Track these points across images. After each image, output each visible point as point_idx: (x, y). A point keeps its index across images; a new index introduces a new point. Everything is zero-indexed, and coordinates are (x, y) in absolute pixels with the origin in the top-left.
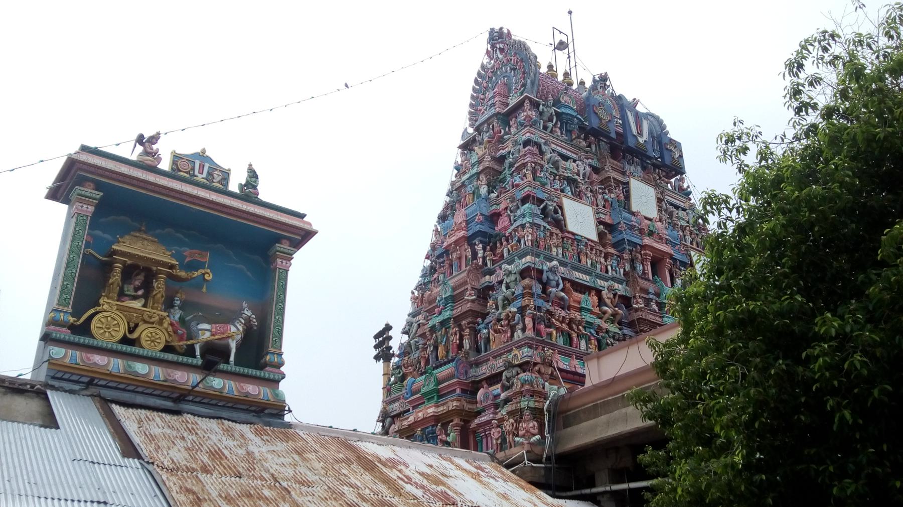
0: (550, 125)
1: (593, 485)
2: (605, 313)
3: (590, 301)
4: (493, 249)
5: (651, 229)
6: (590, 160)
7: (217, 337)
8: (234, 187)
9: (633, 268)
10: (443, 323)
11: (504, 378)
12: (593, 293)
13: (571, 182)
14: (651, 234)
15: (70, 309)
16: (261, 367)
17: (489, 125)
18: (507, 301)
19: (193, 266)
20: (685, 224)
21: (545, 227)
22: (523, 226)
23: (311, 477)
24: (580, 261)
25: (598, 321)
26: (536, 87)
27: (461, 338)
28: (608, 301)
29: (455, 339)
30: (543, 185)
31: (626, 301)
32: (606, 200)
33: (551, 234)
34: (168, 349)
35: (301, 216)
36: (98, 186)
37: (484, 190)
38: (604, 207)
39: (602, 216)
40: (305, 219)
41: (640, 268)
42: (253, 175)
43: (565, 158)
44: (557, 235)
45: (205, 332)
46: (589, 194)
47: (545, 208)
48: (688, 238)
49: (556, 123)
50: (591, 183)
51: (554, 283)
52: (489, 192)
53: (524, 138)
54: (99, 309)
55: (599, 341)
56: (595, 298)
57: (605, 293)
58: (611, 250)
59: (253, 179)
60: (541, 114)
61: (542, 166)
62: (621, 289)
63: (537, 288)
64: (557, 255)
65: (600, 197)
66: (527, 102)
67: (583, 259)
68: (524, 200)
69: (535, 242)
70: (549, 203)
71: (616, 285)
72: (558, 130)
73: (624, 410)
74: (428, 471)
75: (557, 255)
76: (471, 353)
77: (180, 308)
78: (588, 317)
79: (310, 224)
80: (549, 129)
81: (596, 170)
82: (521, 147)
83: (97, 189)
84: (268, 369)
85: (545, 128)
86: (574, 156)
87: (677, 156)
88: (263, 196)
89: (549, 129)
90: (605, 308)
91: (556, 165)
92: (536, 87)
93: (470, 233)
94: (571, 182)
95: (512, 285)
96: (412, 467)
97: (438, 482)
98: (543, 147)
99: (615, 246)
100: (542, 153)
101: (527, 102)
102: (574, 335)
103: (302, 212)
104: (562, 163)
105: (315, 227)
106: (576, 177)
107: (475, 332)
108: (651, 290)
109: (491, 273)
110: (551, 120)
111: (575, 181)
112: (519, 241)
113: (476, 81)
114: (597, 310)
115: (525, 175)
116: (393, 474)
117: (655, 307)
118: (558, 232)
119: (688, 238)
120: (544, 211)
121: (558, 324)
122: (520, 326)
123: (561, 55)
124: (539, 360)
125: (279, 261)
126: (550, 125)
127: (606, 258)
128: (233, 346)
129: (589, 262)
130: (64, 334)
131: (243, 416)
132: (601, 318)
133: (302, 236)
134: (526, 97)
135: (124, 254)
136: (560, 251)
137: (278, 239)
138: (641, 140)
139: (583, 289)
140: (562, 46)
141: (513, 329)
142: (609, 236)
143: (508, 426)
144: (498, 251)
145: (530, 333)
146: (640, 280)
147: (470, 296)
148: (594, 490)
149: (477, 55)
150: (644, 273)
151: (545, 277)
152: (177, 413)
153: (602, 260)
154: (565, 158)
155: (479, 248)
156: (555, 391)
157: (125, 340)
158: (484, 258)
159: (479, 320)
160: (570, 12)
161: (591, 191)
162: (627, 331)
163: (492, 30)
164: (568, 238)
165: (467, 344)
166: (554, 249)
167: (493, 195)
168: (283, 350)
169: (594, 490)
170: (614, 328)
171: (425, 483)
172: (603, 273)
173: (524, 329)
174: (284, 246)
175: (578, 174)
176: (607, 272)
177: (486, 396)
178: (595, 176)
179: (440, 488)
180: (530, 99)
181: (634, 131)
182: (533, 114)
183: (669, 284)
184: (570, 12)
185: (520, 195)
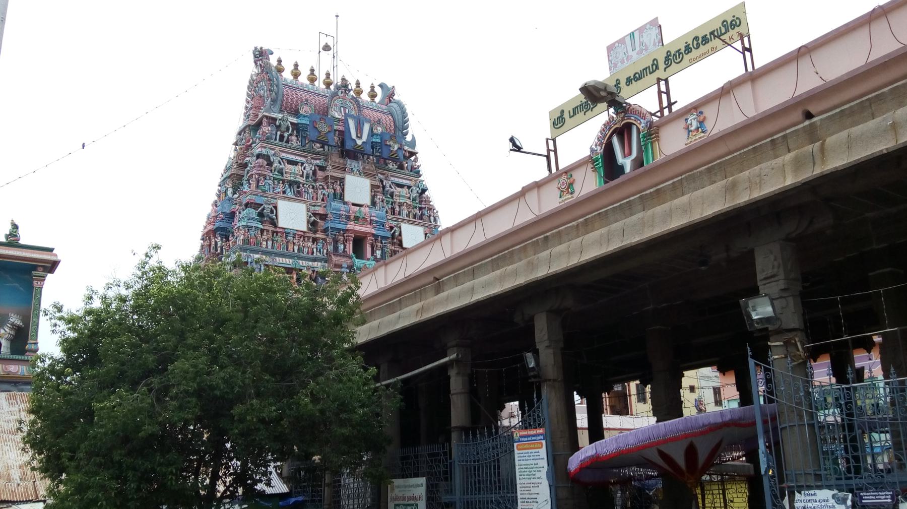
5: (358, 215)
6: (318, 161)
9: (336, 248)
13: (291, 184)
14: (356, 218)
21: (256, 228)
24: (287, 249)
26: (279, 102)
30: (264, 192)
33: (262, 231)
35: (51, 250)
37: (230, 191)
38: (323, 200)
39: (317, 208)
40: (54, 252)
41: (341, 247)
44: (268, 231)
46: (311, 190)
47: (264, 209)
48: (405, 212)
49: (293, 131)
50: (315, 181)
52: (234, 193)
60: (278, 127)
64: (267, 247)
65: (320, 192)
67: (290, 247)
68: (247, 205)
69: (247, 241)
72: (294, 138)
75: (267, 247)
79: (56, 255)
80: (285, 139)
81: (322, 168)
84: (28, 354)
85: (282, 137)
86: (303, 159)
87: (396, 148)
89: (285, 139)
91: (281, 172)
92: (279, 102)
93: (215, 227)
100: (270, 164)
103: (50, 247)
105: (59, 258)
111: (298, 184)
113: (248, 88)
118: (271, 228)
119: (405, 212)
120: (261, 215)
123: (327, 56)
125: (35, 282)
126: (286, 135)
129: (296, 248)
133: (52, 266)
136: (270, 243)
137: (35, 268)
138: (359, 142)
140: (327, 48)
149: (250, 69)
153: (310, 244)
158: (222, 248)
160: (337, 16)
161: (313, 188)
163: (256, 48)
167: (236, 196)
168: (39, 340)
172: (310, 255)
174: (39, 273)
175: (302, 176)
176: (313, 253)
184: (337, 16)
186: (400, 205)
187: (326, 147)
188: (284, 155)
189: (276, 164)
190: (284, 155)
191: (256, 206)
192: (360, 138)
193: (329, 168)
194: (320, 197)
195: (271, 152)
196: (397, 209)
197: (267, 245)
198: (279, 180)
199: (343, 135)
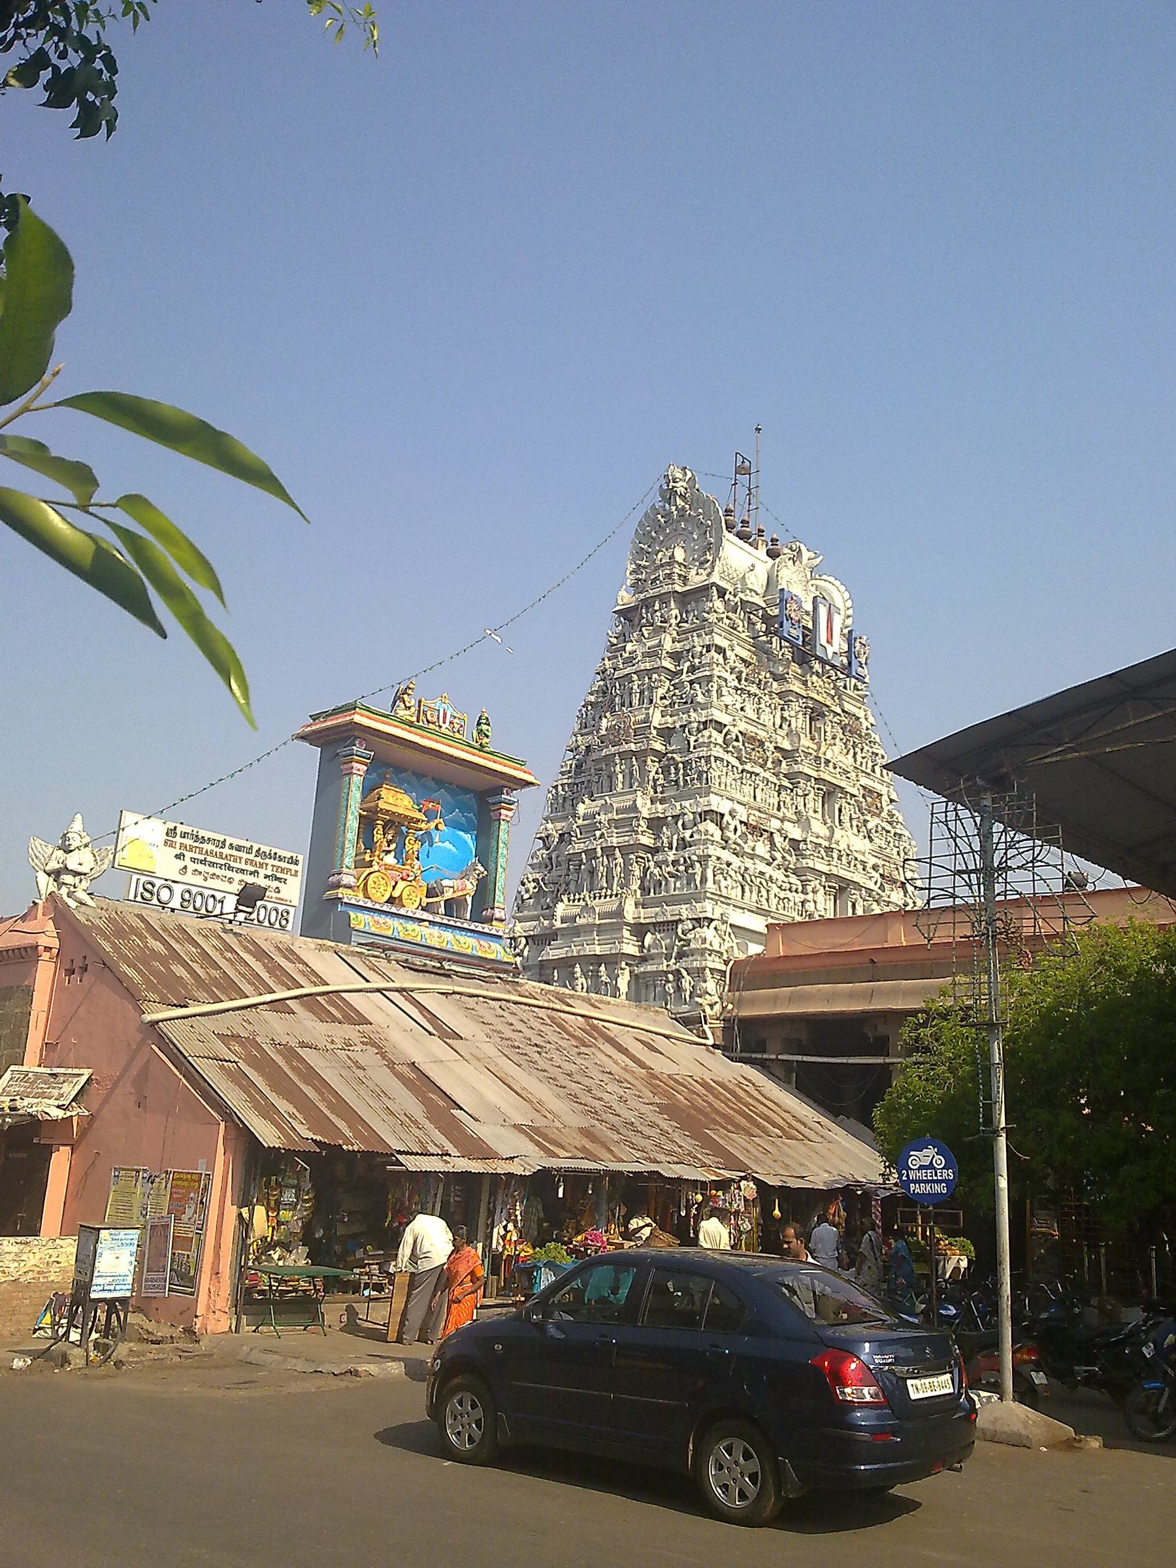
7: (460, 894)
16: (489, 920)
17: (661, 602)
19: (430, 815)
22: (708, 759)
32: (782, 718)
54: (372, 870)
57: (778, 839)
58: (786, 783)
62: (795, 833)
70: (732, 728)
71: (787, 826)
76: (639, 892)
98: (728, 653)
114: (767, 856)
132: (769, 864)
134: (714, 584)
151: (725, 821)
157: (391, 900)
164: (748, 772)
170: (779, 875)
177: (656, 944)
180: (718, 587)
182: (718, 604)
188: (738, 650)
190: (738, 650)
198: (737, 689)
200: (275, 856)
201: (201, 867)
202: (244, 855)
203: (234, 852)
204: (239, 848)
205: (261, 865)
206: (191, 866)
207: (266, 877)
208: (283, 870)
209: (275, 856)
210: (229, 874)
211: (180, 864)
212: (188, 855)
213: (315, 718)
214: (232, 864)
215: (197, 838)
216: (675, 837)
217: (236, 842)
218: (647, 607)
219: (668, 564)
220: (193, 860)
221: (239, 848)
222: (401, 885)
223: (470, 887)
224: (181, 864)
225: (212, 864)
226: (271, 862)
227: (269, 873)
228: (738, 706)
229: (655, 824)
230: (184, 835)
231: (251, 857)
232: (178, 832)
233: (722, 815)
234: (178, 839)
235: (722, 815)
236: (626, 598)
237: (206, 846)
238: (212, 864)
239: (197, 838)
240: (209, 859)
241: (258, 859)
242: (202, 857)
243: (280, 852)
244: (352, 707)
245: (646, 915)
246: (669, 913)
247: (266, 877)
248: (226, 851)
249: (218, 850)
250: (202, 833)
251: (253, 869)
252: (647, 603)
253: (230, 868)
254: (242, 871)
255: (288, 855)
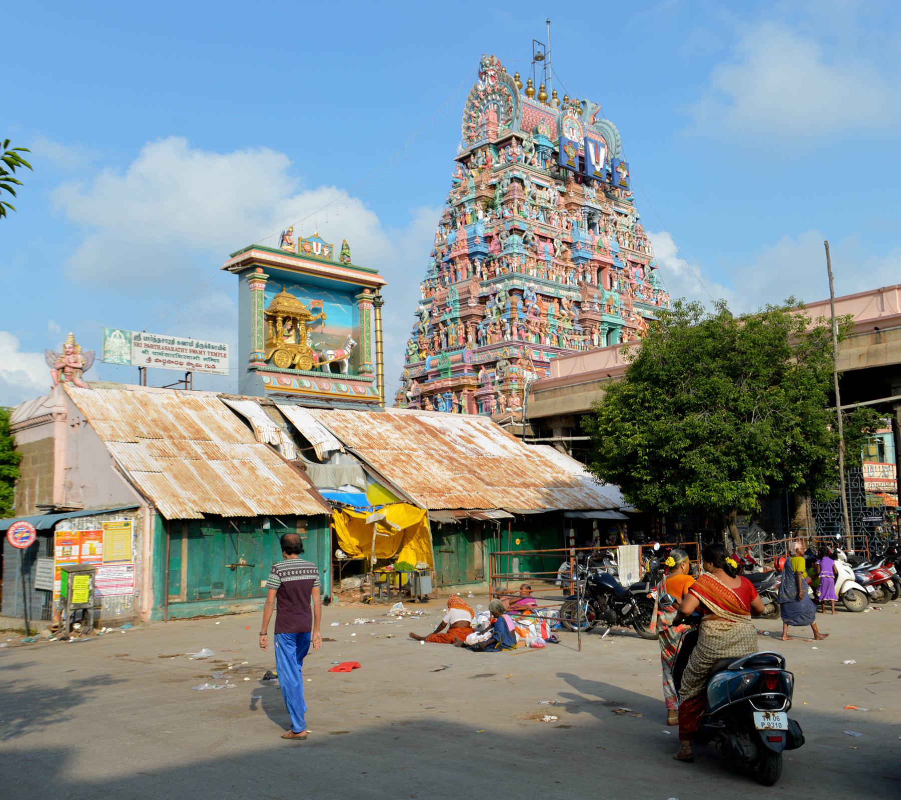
0: (530, 156)
1: (551, 436)
2: (563, 315)
3: (553, 307)
4: (488, 265)
8: (336, 258)
9: (585, 278)
10: (452, 320)
11: (498, 367)
12: (556, 300)
13: (544, 209)
15: (263, 351)
16: (359, 373)
18: (500, 312)
20: (625, 230)
22: (511, 254)
23: (415, 446)
25: (558, 323)
27: (466, 333)
28: (565, 306)
29: (462, 333)
31: (578, 304)
34: (313, 368)
36: (266, 271)
37: (480, 214)
39: (565, 237)
42: (345, 246)
43: (540, 187)
45: (331, 355)
46: (557, 217)
48: (627, 242)
51: (530, 298)
53: (511, 175)
55: (558, 337)
56: (558, 305)
57: (564, 301)
58: (571, 265)
59: (347, 251)
61: (524, 201)
63: (520, 304)
65: (564, 219)
66: (514, 140)
68: (511, 232)
71: (571, 293)
73: (572, 396)
74: (461, 433)
77: (311, 338)
78: (552, 321)
82: (509, 181)
83: (265, 273)
88: (354, 262)
89: (529, 161)
90: (563, 311)
94: (544, 209)
95: (503, 299)
96: (454, 432)
97: (470, 442)
98: (526, 182)
99: (572, 260)
101: (514, 140)
102: (542, 335)
104: (539, 193)
106: (548, 205)
107: (477, 331)
108: (596, 296)
109: (488, 285)
110: (531, 150)
112: (508, 266)
114: (557, 314)
115: (512, 209)
116: (448, 439)
117: (597, 308)
118: (534, 256)
120: (525, 242)
121: (532, 328)
122: (509, 331)
124: (520, 356)
127: (566, 271)
128: (346, 361)
129: (554, 276)
130: (262, 366)
131: (361, 408)
135: (283, 312)
137: (361, 290)
138: (598, 169)
139: (549, 298)
141: (504, 333)
142: (569, 252)
143: (502, 398)
144: (492, 269)
145: (516, 338)
146: (589, 289)
147: (473, 303)
148: (552, 439)
150: (592, 282)
151: (525, 295)
152: (332, 409)
153: (564, 273)
154: (540, 187)
155: (478, 264)
156: (530, 376)
157: (293, 366)
159: (479, 321)
162: (578, 327)
165: (471, 338)
166: (531, 271)
167: (487, 219)
169: (552, 439)
170: (568, 325)
171: (464, 443)
172: (564, 284)
173: (512, 334)
175: (549, 202)
177: (485, 376)
178: (562, 199)
179: (472, 446)
181: (594, 163)
183: (609, 287)
185: (509, 226)
186: (624, 234)
187: (561, 170)
188: (533, 179)
189: (528, 189)
190: (533, 179)
191: (521, 232)
192: (597, 163)
193: (572, 194)
194: (565, 224)
195: (524, 176)
196: (621, 239)
197: (533, 273)
198: (533, 206)
199: (583, 161)
200: (209, 346)
201: (160, 357)
202: (188, 348)
203: (181, 346)
204: (184, 344)
205: (201, 352)
206: (154, 357)
207: (205, 359)
208: (216, 354)
209: (209, 346)
210: (179, 360)
211: (146, 356)
212: (151, 350)
213: (233, 256)
214: (181, 354)
215: (155, 340)
216: (495, 308)
217: (182, 340)
218: (474, 155)
219: (487, 124)
220: (154, 353)
221: (184, 344)
222: (298, 358)
223: (347, 351)
224: (146, 356)
225: (167, 355)
226: (207, 350)
227: (207, 356)
228: (534, 217)
229: (483, 300)
230: (146, 339)
231: (193, 348)
232: (142, 337)
233: (523, 291)
234: (143, 342)
235: (523, 291)
236: (462, 150)
237: (161, 344)
238: (167, 355)
239: (155, 340)
240: (165, 352)
241: (198, 349)
242: (159, 351)
243: (212, 344)
244: (252, 248)
245: (478, 359)
246: (491, 356)
247: (205, 359)
248: (176, 346)
249: (170, 346)
250: (158, 336)
251: (195, 355)
252: (473, 152)
253: (180, 356)
254: (188, 357)
255: (218, 345)
